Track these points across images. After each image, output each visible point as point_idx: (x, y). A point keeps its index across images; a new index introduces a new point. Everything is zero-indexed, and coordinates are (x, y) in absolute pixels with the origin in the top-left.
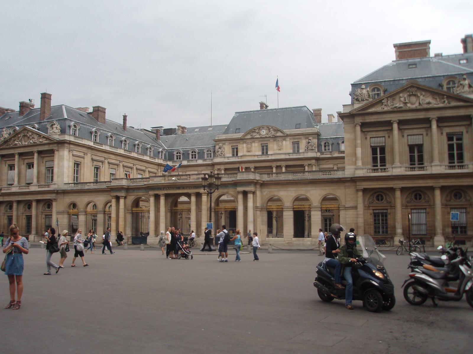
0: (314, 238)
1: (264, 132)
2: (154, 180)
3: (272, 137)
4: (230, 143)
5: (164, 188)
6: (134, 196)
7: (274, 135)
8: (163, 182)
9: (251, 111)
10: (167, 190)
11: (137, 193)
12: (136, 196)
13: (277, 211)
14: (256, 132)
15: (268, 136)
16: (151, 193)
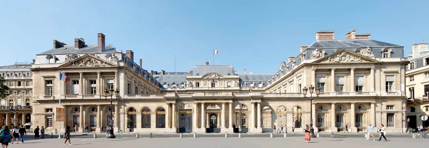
1: (213, 76)
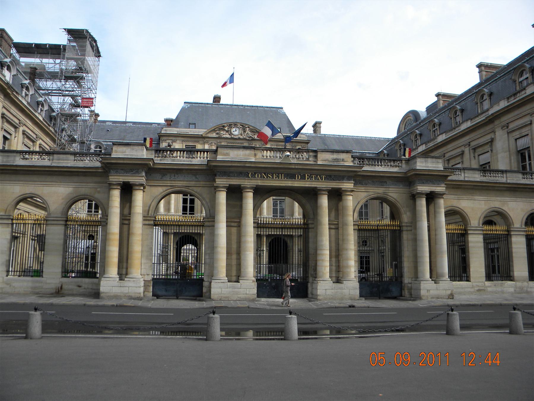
0: (517, 281)
1: (236, 132)
2: (228, 154)
3: (248, 140)
4: (183, 141)
5: (255, 173)
6: (165, 188)
7: (251, 137)
8: (253, 160)
9: (208, 104)
10: (264, 177)
11: (173, 182)
12: (169, 188)
13: (484, 234)
14: (225, 130)
15: (241, 137)
16: (220, 181)
